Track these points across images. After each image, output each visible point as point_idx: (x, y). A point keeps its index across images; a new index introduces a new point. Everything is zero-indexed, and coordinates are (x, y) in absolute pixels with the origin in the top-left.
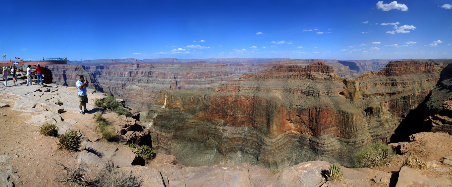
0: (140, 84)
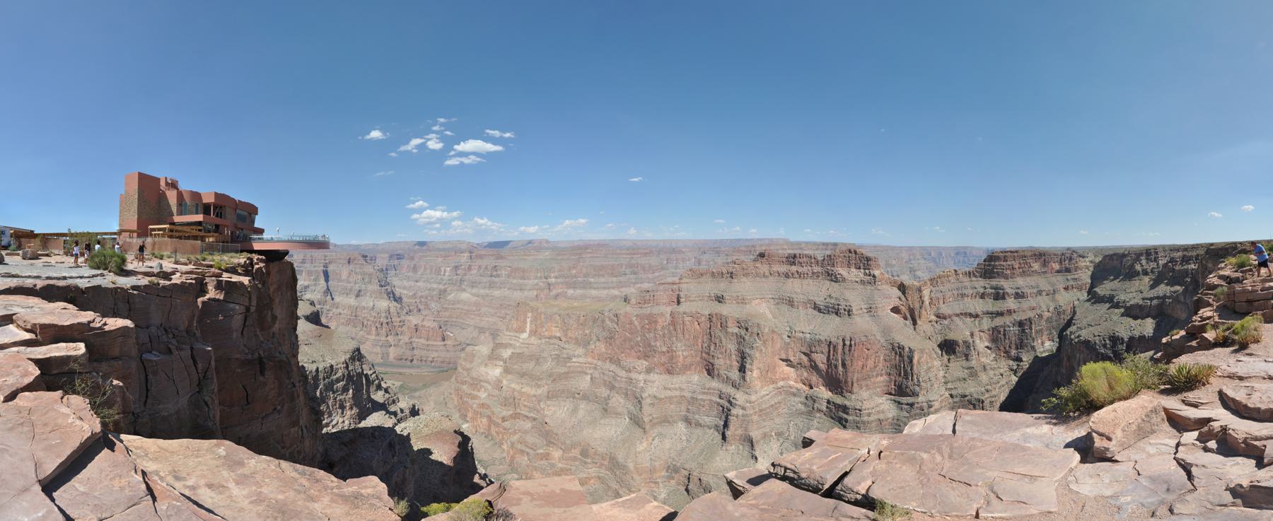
0: (475, 291)
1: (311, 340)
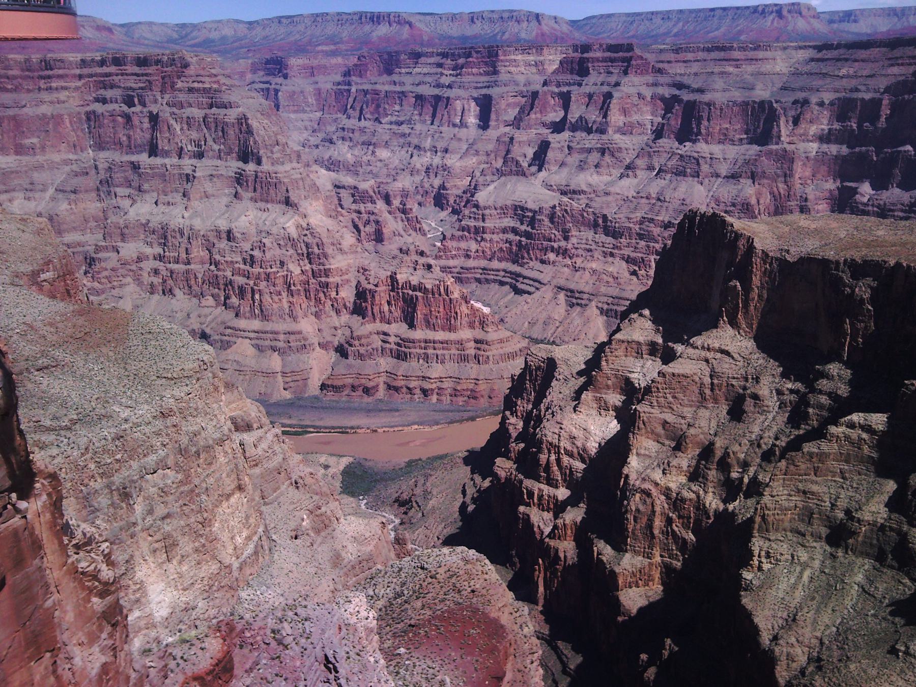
1: (58, 353)
